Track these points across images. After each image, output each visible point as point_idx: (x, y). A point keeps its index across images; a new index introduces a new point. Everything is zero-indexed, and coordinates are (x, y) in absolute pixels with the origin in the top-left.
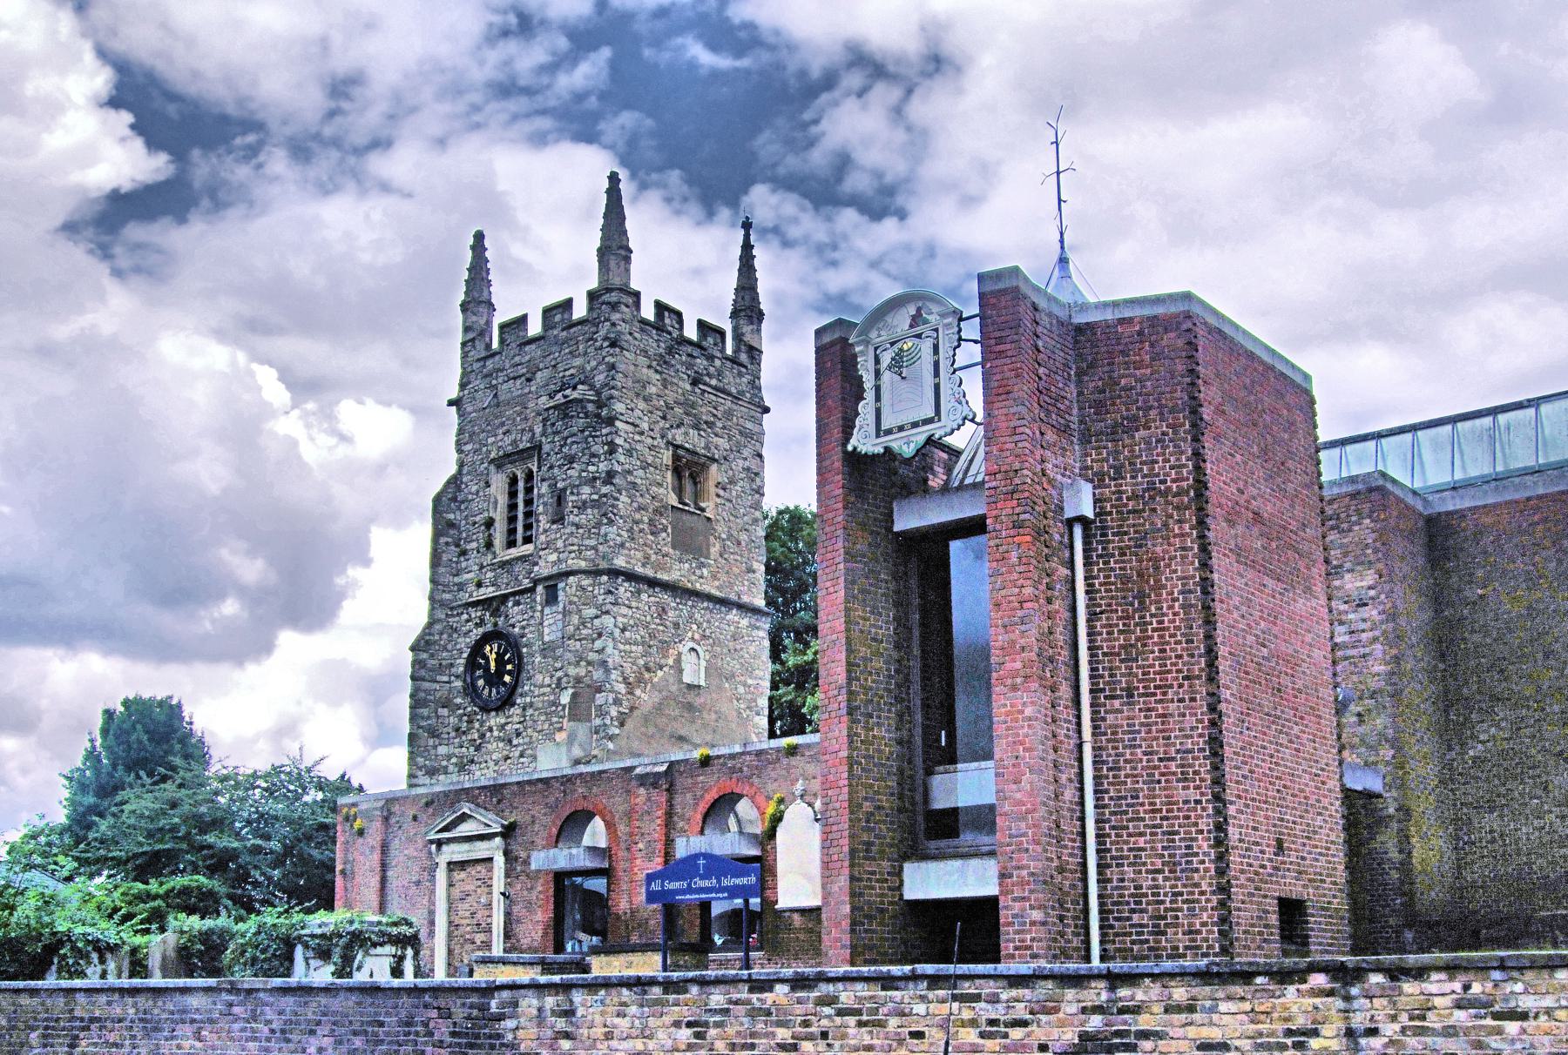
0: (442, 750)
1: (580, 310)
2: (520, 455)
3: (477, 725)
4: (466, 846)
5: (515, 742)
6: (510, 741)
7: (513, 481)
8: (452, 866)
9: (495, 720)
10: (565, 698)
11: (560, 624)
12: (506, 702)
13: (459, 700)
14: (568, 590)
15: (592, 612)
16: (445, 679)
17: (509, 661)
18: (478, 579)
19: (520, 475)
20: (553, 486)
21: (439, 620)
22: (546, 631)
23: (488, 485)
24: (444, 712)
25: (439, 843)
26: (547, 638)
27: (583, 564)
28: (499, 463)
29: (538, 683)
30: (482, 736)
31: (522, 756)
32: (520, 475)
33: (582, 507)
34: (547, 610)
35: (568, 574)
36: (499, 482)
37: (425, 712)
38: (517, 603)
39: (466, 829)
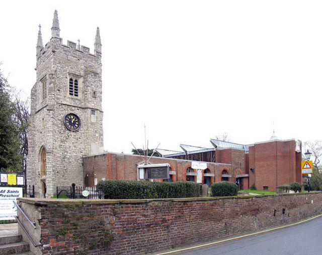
1: (92, 52)
2: (74, 75)
6: (77, 139)
7: (71, 80)
19: (74, 80)
28: (70, 74)
29: (82, 129)
30: (69, 136)
32: (74, 80)
34: (92, 115)
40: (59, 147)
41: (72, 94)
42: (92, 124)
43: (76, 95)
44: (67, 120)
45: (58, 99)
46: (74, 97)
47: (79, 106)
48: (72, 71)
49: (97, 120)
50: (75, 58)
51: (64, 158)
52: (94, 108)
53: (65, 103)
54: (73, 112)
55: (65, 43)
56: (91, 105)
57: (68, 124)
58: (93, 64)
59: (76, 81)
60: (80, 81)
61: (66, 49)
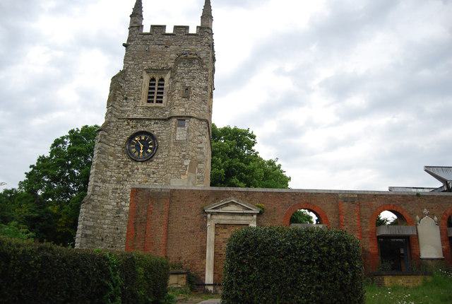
0: (109, 173)
2: (156, 71)
3: (129, 166)
4: (229, 217)
5: (152, 176)
6: (149, 175)
7: (153, 79)
8: (218, 226)
9: (140, 166)
10: (187, 163)
11: (185, 135)
12: (148, 159)
13: (119, 155)
14: (189, 124)
15: (197, 133)
16: (113, 145)
17: (151, 144)
18: (138, 107)
19: (157, 79)
20: (184, 86)
21: (113, 122)
22: (178, 136)
23: (142, 78)
24: (111, 158)
25: (212, 214)
26: (177, 139)
27: (196, 116)
28: (148, 71)
30: (133, 171)
31: (155, 182)
32: (157, 79)
33: (197, 95)
35: (191, 117)
36: (146, 78)
37: (104, 156)
38: (157, 123)
39: (232, 209)
40: (113, 192)
41: (153, 102)
42: (177, 143)
43: (157, 102)
44: (133, 143)
45: (123, 112)
46: (154, 104)
47: (161, 117)
48: (153, 65)
49: (188, 136)
50: (160, 47)
51: (118, 212)
52: (183, 114)
53: (135, 116)
54: (146, 129)
55: (147, 29)
56: (179, 111)
57: (134, 150)
58: (193, 47)
59: (162, 80)
60: (167, 77)
61: (146, 37)
